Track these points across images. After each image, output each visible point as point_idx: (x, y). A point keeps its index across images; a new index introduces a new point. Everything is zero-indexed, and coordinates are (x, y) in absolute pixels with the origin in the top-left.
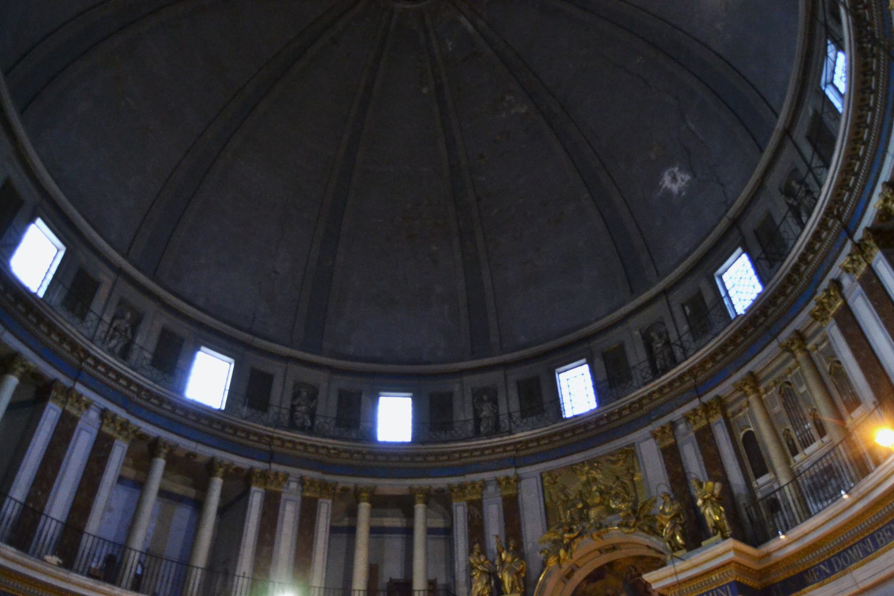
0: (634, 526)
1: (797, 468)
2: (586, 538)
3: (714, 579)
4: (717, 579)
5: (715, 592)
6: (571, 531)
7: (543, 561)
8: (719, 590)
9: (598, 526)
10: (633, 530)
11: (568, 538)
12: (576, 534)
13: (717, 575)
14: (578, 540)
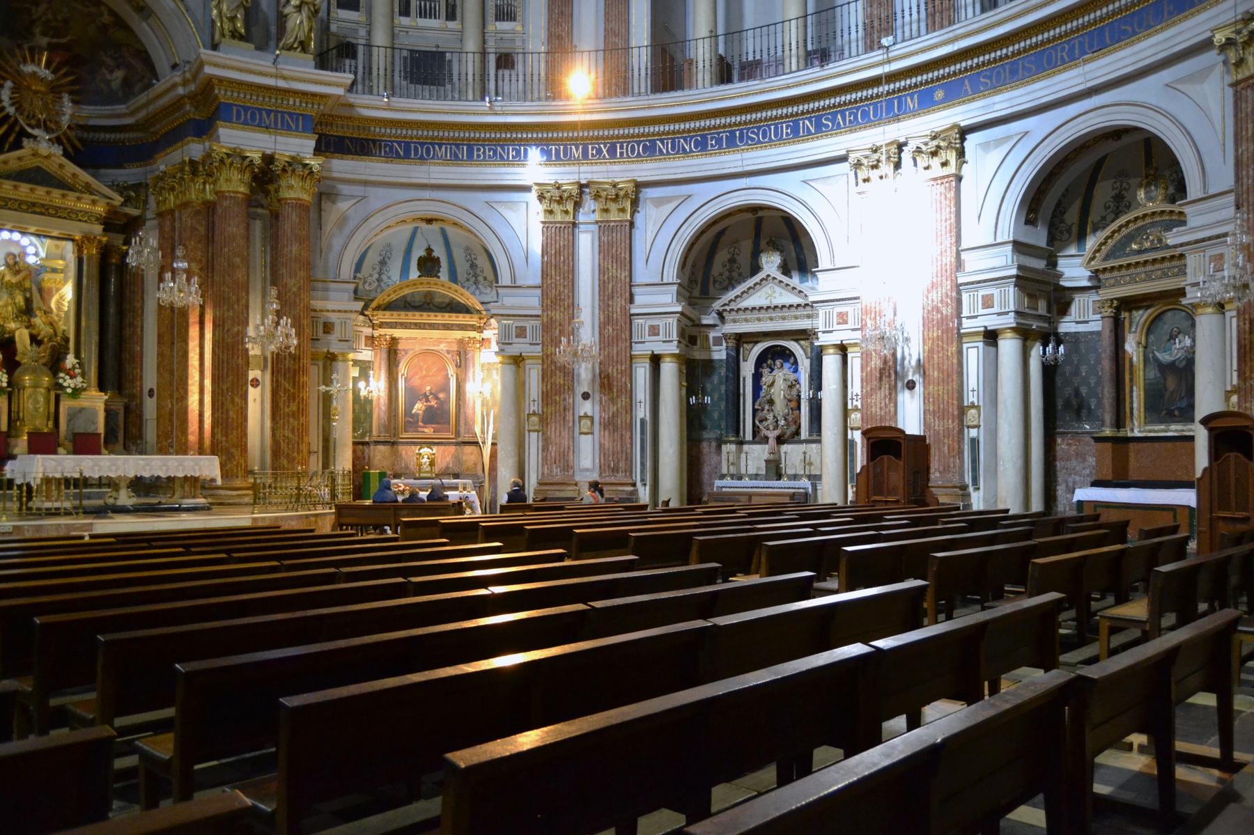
1: (400, 31)
3: (291, 102)
5: (279, 115)
8: (286, 116)
13: (298, 100)
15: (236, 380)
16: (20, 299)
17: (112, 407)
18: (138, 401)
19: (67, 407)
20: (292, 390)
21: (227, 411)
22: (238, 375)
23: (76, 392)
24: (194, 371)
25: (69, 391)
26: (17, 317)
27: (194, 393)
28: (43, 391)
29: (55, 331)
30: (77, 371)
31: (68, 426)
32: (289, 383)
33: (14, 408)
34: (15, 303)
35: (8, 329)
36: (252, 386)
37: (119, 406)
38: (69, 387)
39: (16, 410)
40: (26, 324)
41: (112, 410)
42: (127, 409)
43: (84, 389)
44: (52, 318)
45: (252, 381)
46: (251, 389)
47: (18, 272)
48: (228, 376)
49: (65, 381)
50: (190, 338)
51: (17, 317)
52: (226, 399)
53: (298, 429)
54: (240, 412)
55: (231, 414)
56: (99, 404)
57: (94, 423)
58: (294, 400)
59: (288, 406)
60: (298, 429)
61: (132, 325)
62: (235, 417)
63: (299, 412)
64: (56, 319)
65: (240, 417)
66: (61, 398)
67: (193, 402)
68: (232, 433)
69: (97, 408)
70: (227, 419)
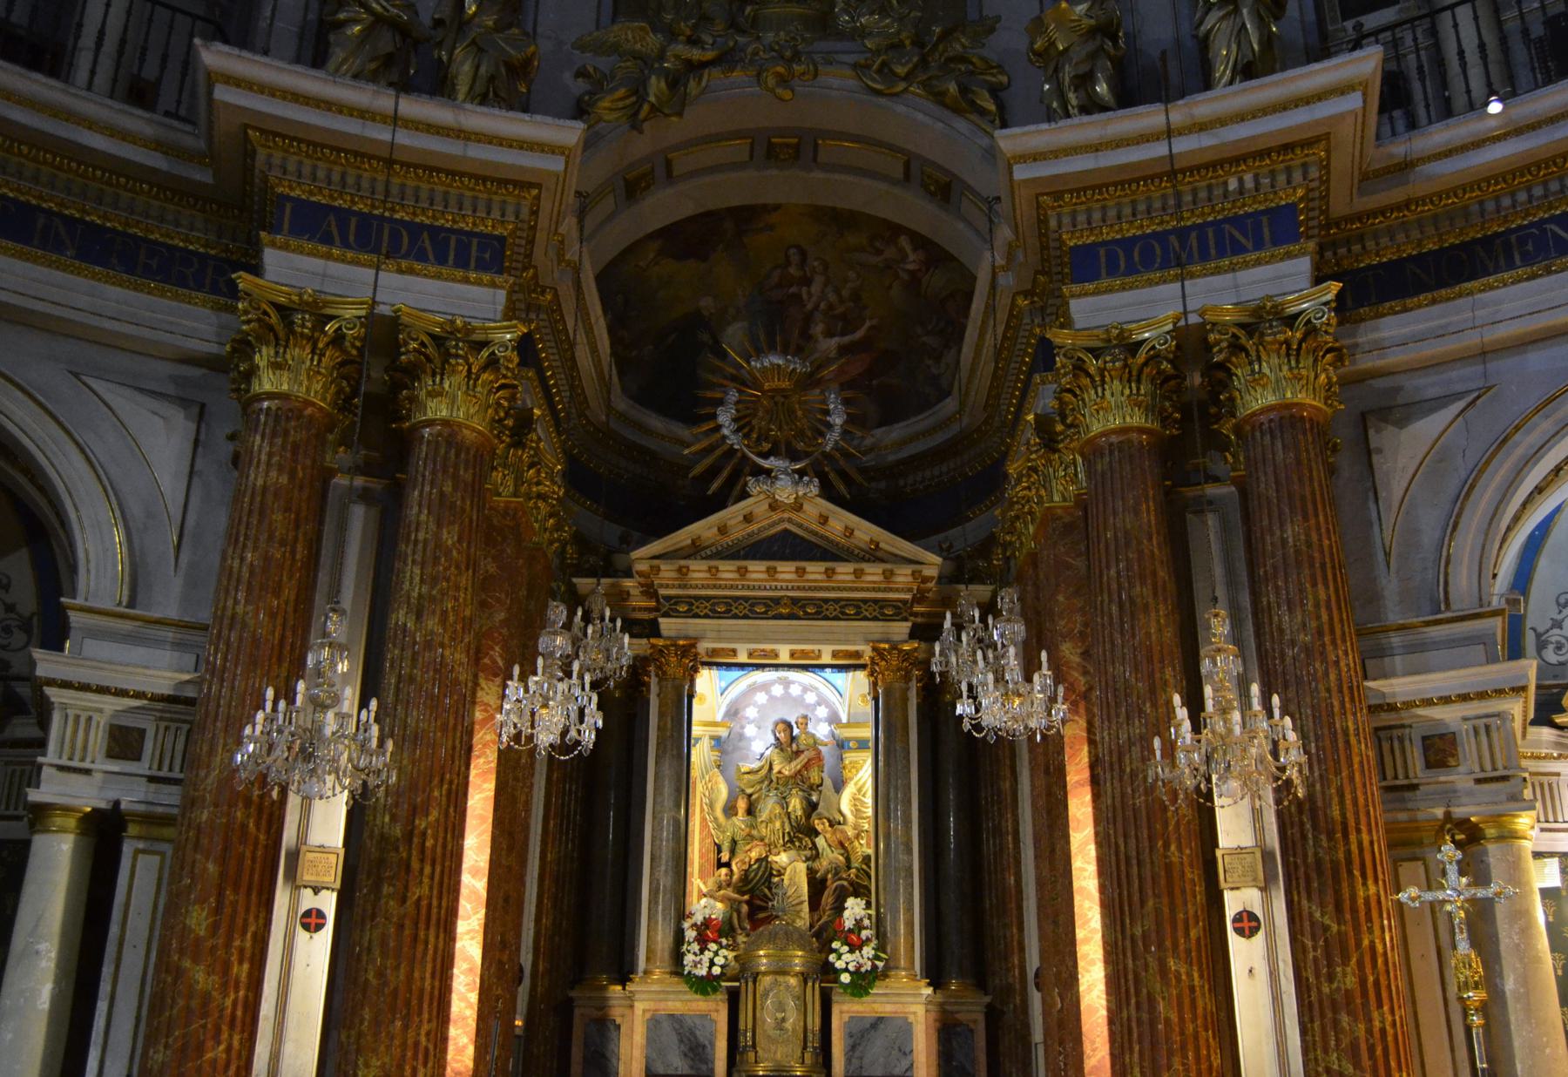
0: (907, 78)
2: (737, 75)
4: (1241, 190)
6: (693, 42)
7: (579, 101)
9: (788, 54)
10: (901, 86)
11: (677, 57)
12: (710, 55)
14: (713, 76)
15: (1166, 910)
16: (796, 804)
17: (958, 1016)
18: (1018, 1000)
19: (846, 1017)
20: (1335, 928)
21: (1151, 1001)
22: (1171, 894)
23: (863, 982)
24: (1087, 904)
25: (845, 978)
26: (791, 841)
27: (1093, 963)
28: (793, 981)
29: (848, 859)
30: (865, 934)
31: (849, 1061)
32: (1322, 905)
33: (745, 1021)
34: (788, 815)
35: (774, 866)
36: (1240, 931)
37: (973, 1011)
38: (846, 970)
39: (750, 1026)
40: (808, 853)
41: (960, 1024)
42: (993, 1016)
43: (885, 975)
44: (843, 832)
45: (1238, 918)
46: (1234, 941)
47: (798, 753)
48: (1143, 903)
49: (839, 958)
50: (1072, 824)
51: (791, 841)
52: (1146, 965)
53: (1371, 1049)
54: (1187, 1001)
55: (1161, 1006)
56: (913, 1008)
57: (906, 1052)
58: (1345, 963)
59: (1331, 978)
60: (1371, 1049)
61: (998, 832)
62: (1174, 1017)
63: (1364, 994)
64: (851, 833)
65: (1188, 1016)
66: (834, 998)
67: (1090, 989)
68: (1169, 1067)
69: (911, 1018)
70: (1153, 1023)
